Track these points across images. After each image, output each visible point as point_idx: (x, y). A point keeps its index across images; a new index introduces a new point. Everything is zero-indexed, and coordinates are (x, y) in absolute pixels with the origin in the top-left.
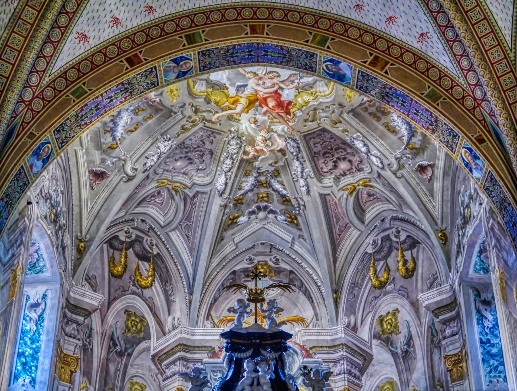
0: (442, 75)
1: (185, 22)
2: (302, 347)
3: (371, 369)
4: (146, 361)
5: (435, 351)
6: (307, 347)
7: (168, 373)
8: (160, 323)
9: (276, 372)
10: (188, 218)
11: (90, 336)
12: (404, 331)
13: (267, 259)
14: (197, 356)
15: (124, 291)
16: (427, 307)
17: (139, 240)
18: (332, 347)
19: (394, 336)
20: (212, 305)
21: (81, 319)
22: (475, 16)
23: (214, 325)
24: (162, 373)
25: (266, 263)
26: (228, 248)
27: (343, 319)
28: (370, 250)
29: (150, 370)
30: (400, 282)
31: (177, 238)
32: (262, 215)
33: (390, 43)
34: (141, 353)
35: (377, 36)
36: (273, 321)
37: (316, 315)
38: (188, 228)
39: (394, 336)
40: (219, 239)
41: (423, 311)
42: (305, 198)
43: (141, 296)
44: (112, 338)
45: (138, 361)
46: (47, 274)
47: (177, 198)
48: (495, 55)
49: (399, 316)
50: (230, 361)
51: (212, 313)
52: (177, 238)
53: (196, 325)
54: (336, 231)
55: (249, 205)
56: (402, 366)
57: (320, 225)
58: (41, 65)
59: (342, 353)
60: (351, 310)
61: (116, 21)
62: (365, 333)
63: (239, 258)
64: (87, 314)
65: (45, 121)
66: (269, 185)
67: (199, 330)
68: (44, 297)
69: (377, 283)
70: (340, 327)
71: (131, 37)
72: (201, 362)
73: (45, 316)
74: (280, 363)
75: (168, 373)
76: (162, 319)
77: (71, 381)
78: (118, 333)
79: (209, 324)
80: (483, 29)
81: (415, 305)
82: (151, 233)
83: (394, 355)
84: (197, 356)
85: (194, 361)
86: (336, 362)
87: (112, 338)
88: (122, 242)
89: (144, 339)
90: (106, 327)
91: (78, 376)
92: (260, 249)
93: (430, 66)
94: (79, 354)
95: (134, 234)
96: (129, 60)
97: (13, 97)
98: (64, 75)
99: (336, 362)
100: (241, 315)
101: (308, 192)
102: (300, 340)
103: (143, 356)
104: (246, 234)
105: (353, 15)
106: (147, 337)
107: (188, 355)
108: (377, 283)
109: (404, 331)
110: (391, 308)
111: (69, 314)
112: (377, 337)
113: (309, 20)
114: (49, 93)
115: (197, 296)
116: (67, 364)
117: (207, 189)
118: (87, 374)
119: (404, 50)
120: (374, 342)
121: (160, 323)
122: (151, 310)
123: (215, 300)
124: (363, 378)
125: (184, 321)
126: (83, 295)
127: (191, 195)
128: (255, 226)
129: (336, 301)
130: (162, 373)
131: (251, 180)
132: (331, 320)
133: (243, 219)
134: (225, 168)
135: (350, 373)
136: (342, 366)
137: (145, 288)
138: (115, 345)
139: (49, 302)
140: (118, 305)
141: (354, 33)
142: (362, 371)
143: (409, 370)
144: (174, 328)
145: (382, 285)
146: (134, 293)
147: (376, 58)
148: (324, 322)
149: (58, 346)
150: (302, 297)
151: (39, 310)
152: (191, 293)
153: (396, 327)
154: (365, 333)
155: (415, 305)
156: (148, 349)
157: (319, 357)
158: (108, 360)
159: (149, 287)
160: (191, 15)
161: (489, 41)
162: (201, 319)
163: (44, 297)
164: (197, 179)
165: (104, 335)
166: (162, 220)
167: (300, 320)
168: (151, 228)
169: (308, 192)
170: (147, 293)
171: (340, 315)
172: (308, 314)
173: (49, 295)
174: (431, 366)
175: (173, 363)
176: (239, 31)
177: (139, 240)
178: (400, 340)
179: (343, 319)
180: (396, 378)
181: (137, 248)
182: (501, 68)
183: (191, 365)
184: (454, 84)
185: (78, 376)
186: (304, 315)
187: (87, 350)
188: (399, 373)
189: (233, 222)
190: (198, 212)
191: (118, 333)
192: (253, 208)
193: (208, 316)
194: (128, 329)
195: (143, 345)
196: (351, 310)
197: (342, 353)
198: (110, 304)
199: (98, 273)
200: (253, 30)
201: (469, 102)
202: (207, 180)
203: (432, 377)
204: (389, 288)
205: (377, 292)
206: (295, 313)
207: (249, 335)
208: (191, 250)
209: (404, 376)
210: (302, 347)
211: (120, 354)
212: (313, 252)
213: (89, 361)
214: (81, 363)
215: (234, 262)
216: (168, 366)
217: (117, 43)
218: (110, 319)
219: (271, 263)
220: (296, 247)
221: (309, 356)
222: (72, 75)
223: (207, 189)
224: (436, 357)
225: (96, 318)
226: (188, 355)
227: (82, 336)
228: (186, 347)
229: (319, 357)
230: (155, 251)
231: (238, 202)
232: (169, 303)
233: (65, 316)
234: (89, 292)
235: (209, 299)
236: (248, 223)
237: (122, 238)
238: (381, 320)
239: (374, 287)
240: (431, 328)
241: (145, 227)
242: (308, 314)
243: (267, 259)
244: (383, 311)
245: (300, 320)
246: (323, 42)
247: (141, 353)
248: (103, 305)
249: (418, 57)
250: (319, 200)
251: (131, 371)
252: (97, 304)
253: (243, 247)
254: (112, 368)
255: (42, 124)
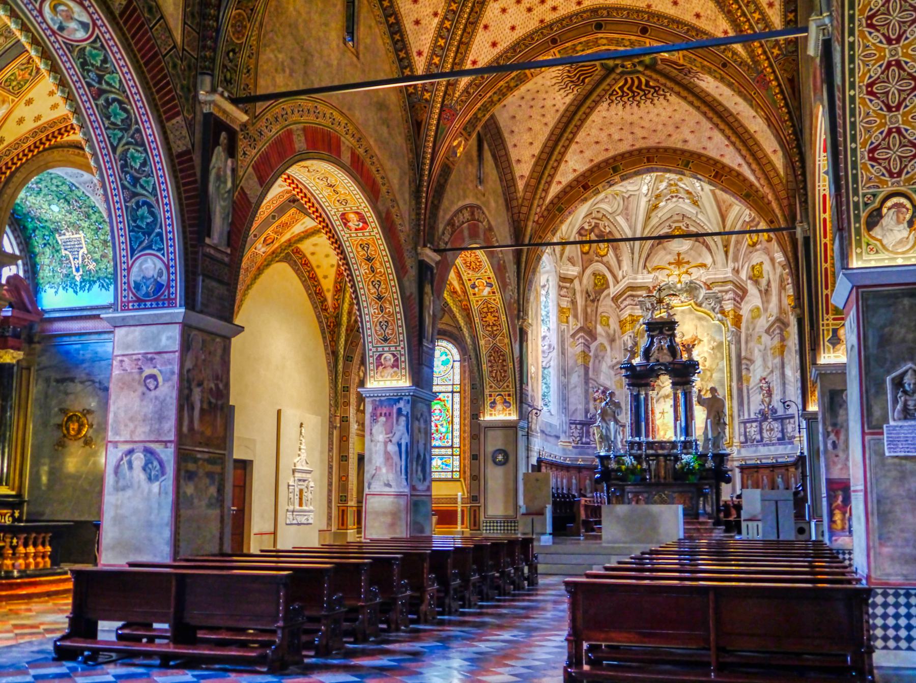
0: (752, 185)
1: (611, 161)
2: (705, 283)
3: (746, 299)
4: (609, 302)
5: (783, 292)
6: (708, 283)
7: (622, 306)
8: (614, 276)
9: (671, 341)
10: (627, 209)
11: (574, 294)
12: (766, 277)
13: (681, 224)
14: (639, 293)
15: (591, 261)
16: (779, 263)
17: (597, 225)
18: (725, 282)
19: (760, 279)
20: (646, 259)
21: (568, 285)
22: (764, 161)
23: (649, 272)
24: (618, 307)
25: (680, 228)
26: (654, 221)
27: (731, 265)
28: (747, 219)
29: (611, 307)
30: (765, 244)
31: (620, 219)
32: (674, 200)
33: (724, 166)
34: (605, 298)
35: (716, 162)
36: (669, 314)
37: (714, 262)
38: (627, 214)
39: (760, 279)
40: (648, 218)
41: (777, 265)
42: (701, 193)
43: (602, 262)
44: (587, 293)
45: (604, 303)
46: (548, 268)
47: (618, 198)
48: (776, 181)
49: (764, 266)
50: (649, 336)
51: (647, 264)
52: (620, 219)
53: (637, 273)
54: (724, 209)
55: (665, 196)
56: (764, 299)
57: (712, 207)
58: (541, 202)
59: (730, 286)
60: (736, 259)
61: (575, 170)
62: (744, 275)
63: (662, 226)
64: (571, 281)
65: (546, 228)
66: (676, 185)
67: (640, 276)
68: (548, 280)
69: (751, 243)
70: (729, 270)
71: (583, 175)
72: (641, 296)
73: (550, 292)
74: (673, 336)
75: (622, 306)
76: (616, 273)
77: (567, 322)
78: (590, 289)
79: (645, 271)
80: (768, 168)
81: (772, 260)
82: (604, 219)
83: (760, 291)
84: (639, 293)
85: (638, 296)
86: (726, 292)
87: (587, 293)
88: (586, 230)
89: (606, 288)
90: (583, 286)
91: (571, 319)
92: (676, 218)
93: (745, 179)
94: (570, 306)
95: (593, 222)
96: (583, 187)
97: (530, 224)
98: (552, 202)
99: (726, 292)
100: (653, 312)
101: (702, 189)
102: (703, 279)
103: (607, 299)
104: (665, 210)
105: (703, 152)
106: (608, 287)
107: (634, 293)
108: (751, 243)
109: (766, 277)
110: (759, 260)
111: (561, 284)
112: (750, 278)
113: (679, 152)
114: (545, 213)
115: (636, 256)
116: (564, 313)
117: (637, 193)
118: (576, 316)
119: (731, 170)
120: (749, 281)
121: (614, 276)
122: (608, 269)
123: (648, 255)
124: (743, 304)
125: (630, 271)
126: (568, 270)
127: (627, 196)
128: (671, 205)
129: (726, 253)
130: (618, 307)
131: (664, 184)
132: (723, 265)
133: (662, 204)
134: (646, 181)
135: (735, 300)
136: (731, 295)
137: (602, 256)
138: (589, 296)
139: (551, 283)
140: (589, 271)
141: (704, 159)
142: (742, 299)
143: (768, 301)
144: (624, 277)
145: (754, 244)
146: (597, 261)
147: (717, 172)
148: (719, 265)
149: (559, 305)
150: (704, 249)
151: (546, 289)
152: (633, 254)
153: (761, 273)
154: (744, 275)
155: (772, 260)
156: (609, 294)
157: (716, 289)
158: (586, 306)
159: (606, 255)
160: (614, 158)
161: (772, 174)
162: (640, 268)
163: (548, 280)
164: (629, 188)
165: (582, 291)
166: (610, 210)
167: (703, 266)
168: (604, 215)
169: (702, 189)
170: (605, 259)
171: (729, 262)
172: (708, 260)
173: (550, 279)
174: (780, 301)
175: (625, 299)
176: (640, 161)
177: (597, 225)
178: (764, 282)
179: (731, 265)
180: (760, 306)
181: (596, 231)
182: (779, 187)
183: (636, 299)
184: (757, 191)
185: (571, 319)
186: (706, 262)
187: (574, 302)
188: (763, 303)
189: (656, 207)
190: (633, 206)
191: (590, 289)
192: (669, 197)
193: (645, 267)
194: (596, 285)
195: (606, 292)
196: (736, 259)
197: (730, 286)
198: (584, 271)
199: (574, 254)
200: (649, 160)
201: (766, 200)
202: (636, 188)
203: (780, 308)
204: (758, 247)
205: (751, 249)
206: (700, 261)
207: (657, 323)
208: (630, 227)
209: (766, 305)
210: (705, 283)
211: (593, 301)
212: (709, 221)
213: (576, 309)
214: (572, 311)
215: (659, 229)
216: (622, 303)
217: (576, 180)
218: (585, 281)
219: (683, 228)
220: (699, 216)
221: (709, 289)
222: (556, 201)
223: (637, 193)
224: (783, 295)
225: (576, 282)
226: (634, 293)
227: (570, 295)
228: (632, 288)
229: (716, 289)
230: (608, 230)
231: (658, 197)
232: (619, 262)
233: (559, 286)
234: (571, 267)
235: (644, 255)
236: (665, 206)
237: (586, 227)
238: (753, 267)
239: (749, 245)
240: (781, 276)
241: (600, 215)
242: (708, 260)
243: (681, 224)
244: (754, 263)
245: (703, 266)
246: (687, 165)
247: (605, 298)
248: (579, 273)
249: (739, 174)
250: (710, 194)
251: (600, 310)
252: (576, 274)
253: (664, 218)
254: (589, 310)
255: (544, 231)
